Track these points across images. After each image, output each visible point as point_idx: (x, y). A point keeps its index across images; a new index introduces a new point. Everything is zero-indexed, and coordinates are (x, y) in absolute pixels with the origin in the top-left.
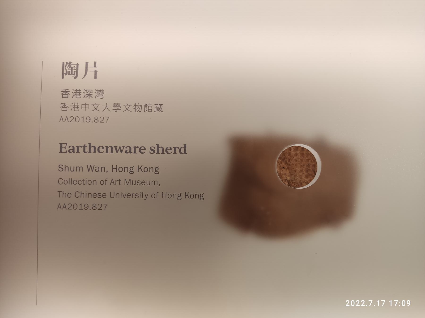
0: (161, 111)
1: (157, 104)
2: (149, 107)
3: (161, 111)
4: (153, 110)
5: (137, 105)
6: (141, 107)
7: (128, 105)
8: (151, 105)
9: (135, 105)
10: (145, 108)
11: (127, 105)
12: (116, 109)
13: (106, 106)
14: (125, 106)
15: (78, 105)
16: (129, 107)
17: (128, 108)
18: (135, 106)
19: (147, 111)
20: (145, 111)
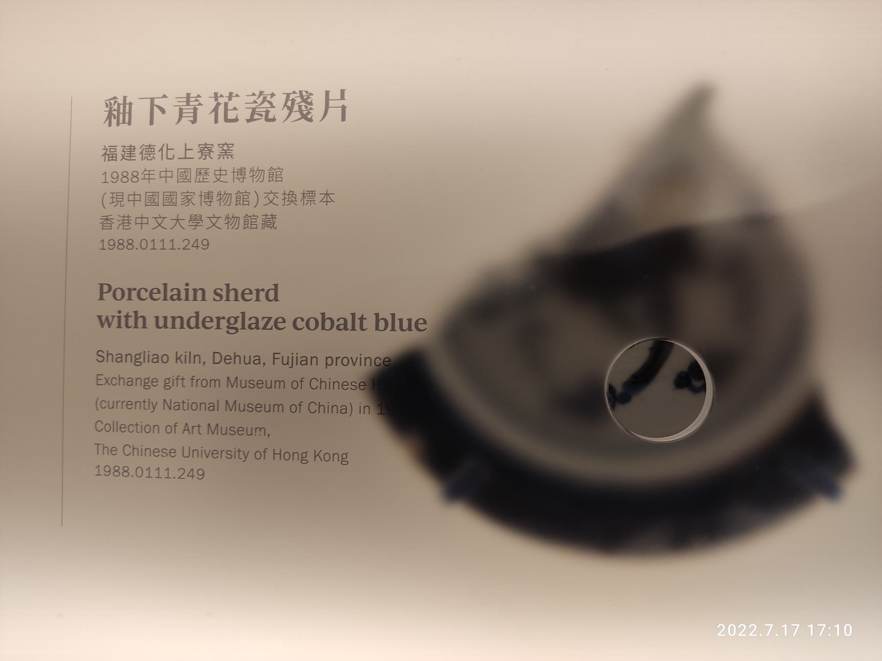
0: (272, 226)
1: (266, 215)
2: (253, 220)
3: (272, 226)
4: (260, 226)
5: (231, 217)
6: (238, 222)
7: (216, 216)
8: (256, 217)
9: (227, 217)
10: (246, 223)
11: (213, 216)
12: (194, 224)
13: (178, 220)
14: (210, 220)
15: (130, 218)
16: (217, 221)
17: (215, 223)
18: (228, 218)
19: (248, 227)
20: (245, 228)
